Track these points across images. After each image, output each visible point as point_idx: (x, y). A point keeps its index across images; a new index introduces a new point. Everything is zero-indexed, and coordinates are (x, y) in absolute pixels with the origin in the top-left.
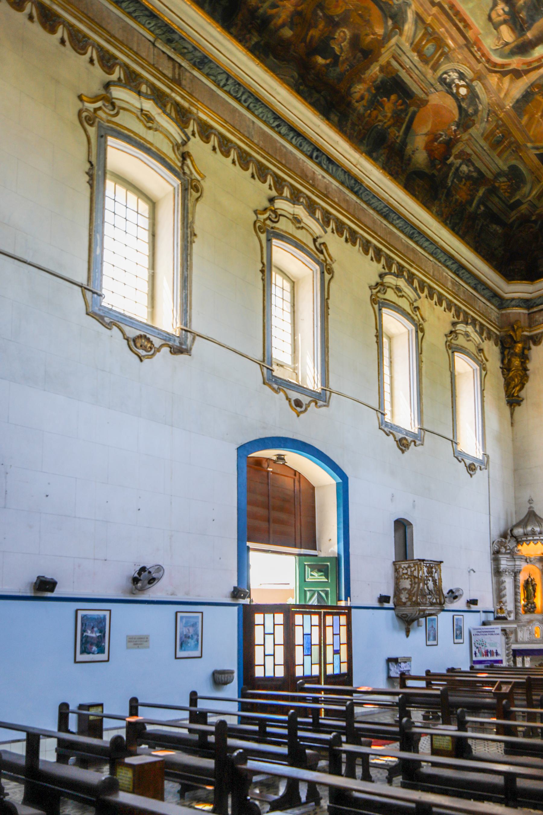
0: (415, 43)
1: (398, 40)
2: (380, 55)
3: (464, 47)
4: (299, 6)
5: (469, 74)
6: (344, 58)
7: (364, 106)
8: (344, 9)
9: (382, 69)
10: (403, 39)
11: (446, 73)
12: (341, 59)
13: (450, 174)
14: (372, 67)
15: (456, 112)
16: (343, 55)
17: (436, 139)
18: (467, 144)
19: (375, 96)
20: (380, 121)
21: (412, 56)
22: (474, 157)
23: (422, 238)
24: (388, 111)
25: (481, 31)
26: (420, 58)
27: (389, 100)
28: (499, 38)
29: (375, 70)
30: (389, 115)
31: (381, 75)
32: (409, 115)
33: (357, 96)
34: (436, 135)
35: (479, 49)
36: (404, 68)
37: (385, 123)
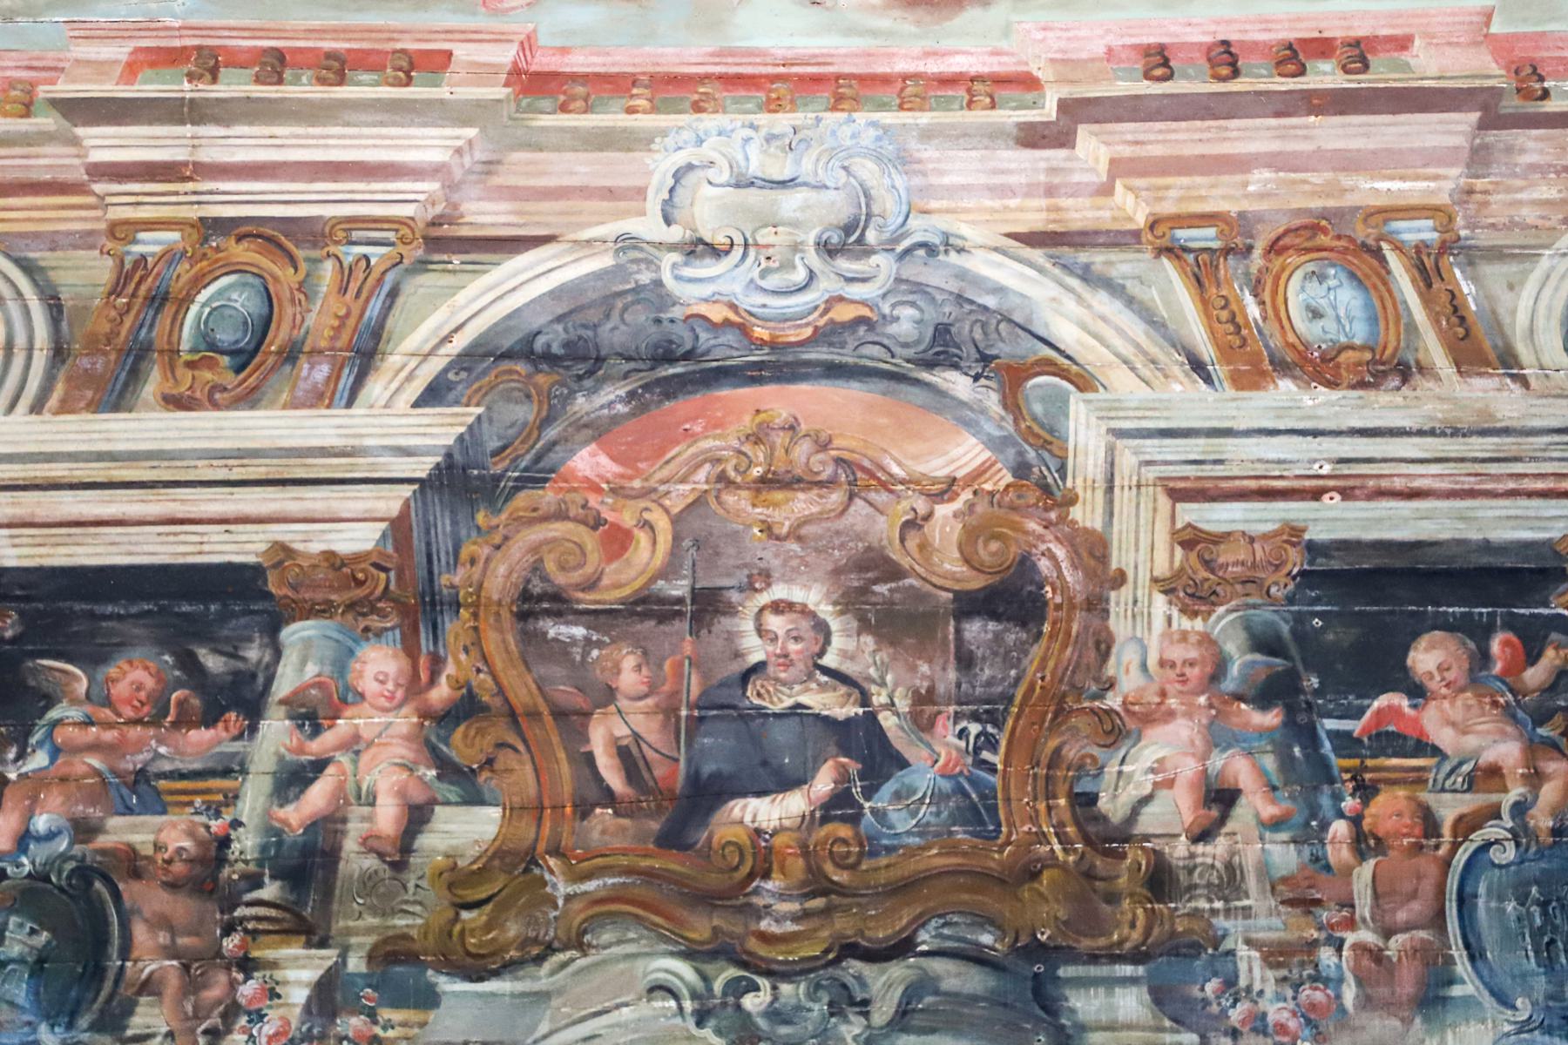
0: (1207, 351)
1: (1108, 411)
3: (1492, 136)
4: (433, 681)
6: (903, 705)
7: (1276, 824)
8: (662, 524)
10: (1123, 384)
12: (887, 721)
14: (1119, 625)
16: (880, 698)
19: (1300, 729)
20: (1466, 826)
21: (1280, 412)
24: (1471, 742)
26: (1332, 385)
27: (1417, 692)
30: (1507, 751)
31: (1223, 623)
36: (1316, 494)
37: (1520, 809)
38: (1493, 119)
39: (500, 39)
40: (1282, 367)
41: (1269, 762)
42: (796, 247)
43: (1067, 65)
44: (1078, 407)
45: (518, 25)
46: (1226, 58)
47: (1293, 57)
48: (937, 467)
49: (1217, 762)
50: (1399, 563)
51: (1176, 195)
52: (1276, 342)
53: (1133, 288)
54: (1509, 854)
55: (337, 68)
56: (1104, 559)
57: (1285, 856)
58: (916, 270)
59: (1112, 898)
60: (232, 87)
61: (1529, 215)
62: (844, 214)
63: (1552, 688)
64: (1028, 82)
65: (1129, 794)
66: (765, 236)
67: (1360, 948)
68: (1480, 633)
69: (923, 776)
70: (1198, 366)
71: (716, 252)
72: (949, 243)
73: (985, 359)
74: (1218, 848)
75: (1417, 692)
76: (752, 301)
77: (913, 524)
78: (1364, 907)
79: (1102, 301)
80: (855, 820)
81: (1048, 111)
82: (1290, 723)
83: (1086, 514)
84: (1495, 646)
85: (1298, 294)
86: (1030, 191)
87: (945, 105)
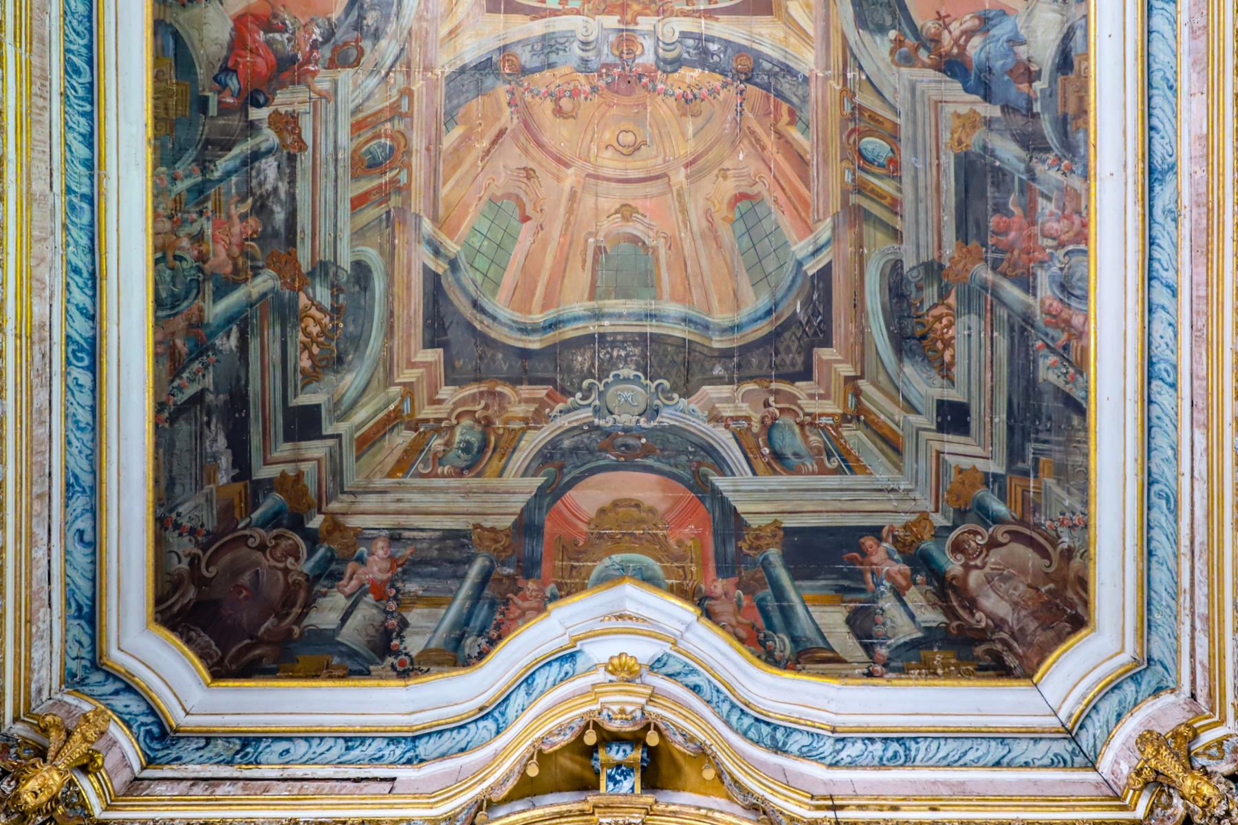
13: (236, 151)
17: (269, 28)
22: (305, 161)
23: (83, 114)
34: (275, 16)
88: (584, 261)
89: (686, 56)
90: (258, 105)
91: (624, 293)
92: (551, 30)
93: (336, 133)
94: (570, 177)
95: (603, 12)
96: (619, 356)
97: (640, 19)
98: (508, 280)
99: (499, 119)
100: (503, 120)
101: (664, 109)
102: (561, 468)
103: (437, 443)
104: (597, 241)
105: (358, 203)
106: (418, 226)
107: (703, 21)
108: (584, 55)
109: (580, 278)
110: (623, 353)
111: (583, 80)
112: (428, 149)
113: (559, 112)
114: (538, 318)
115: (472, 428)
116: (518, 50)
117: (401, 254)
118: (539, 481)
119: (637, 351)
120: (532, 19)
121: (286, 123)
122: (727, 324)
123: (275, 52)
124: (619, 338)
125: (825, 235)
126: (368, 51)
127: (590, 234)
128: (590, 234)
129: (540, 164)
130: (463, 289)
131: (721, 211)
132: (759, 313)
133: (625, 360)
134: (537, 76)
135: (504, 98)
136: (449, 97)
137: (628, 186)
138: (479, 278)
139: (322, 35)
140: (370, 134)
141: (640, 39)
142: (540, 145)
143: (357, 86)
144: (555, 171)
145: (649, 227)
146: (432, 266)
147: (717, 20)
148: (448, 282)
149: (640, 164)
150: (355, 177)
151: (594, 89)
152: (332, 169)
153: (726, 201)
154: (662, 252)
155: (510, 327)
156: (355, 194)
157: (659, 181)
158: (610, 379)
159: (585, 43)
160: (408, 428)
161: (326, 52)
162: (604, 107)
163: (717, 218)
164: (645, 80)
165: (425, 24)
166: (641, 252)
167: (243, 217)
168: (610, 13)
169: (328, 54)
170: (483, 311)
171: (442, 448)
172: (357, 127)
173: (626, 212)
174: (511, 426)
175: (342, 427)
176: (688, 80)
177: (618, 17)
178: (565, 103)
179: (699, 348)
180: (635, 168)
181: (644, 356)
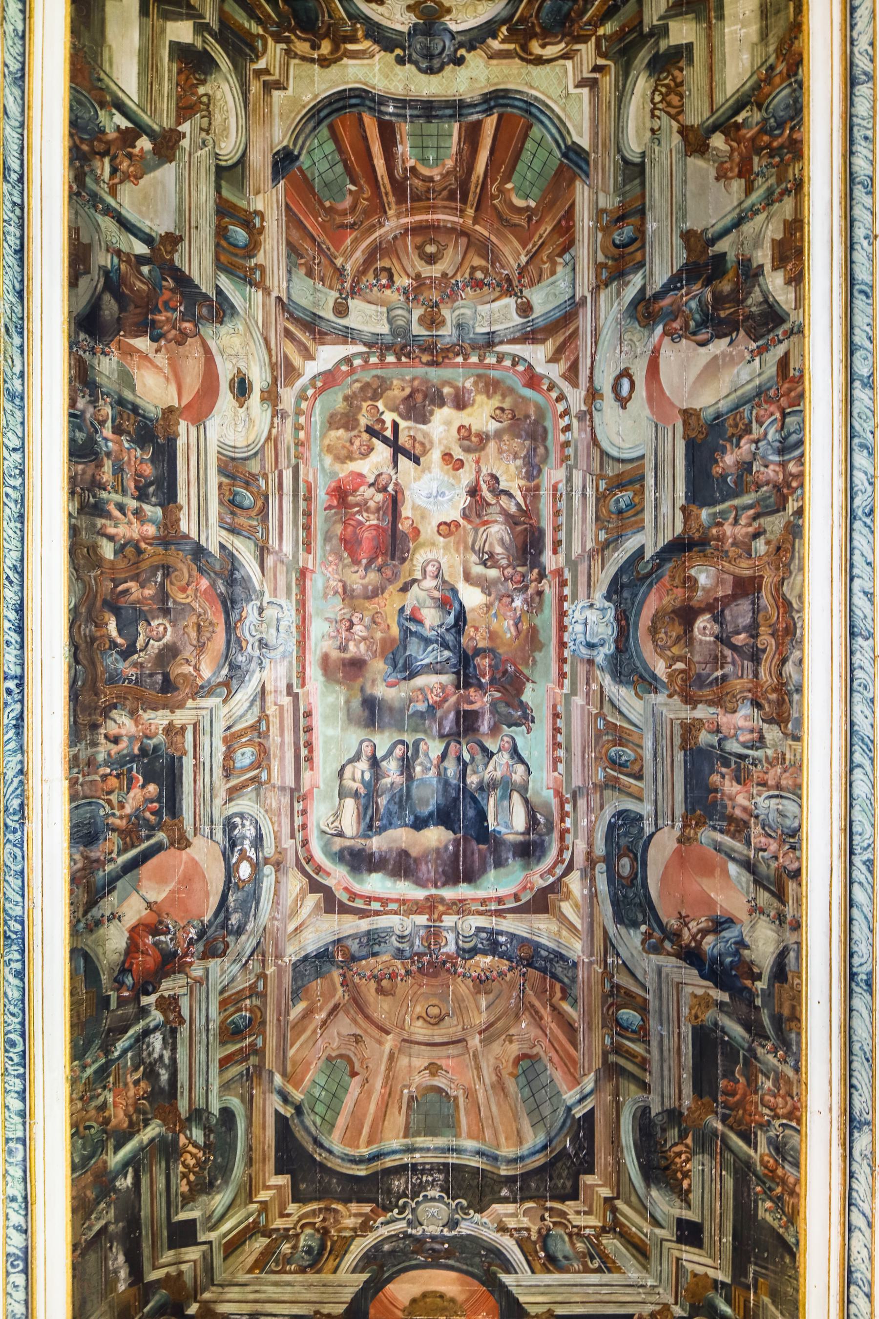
0: (233, 730)
1: (217, 707)
2: (181, 705)
3: (288, 791)
5: (269, 849)
6: (140, 660)
7: (109, 755)
9: (169, 729)
10: (224, 710)
11: (242, 816)
14: (161, 712)
15: (214, 901)
17: (155, 932)
18: (191, 987)
19: (133, 758)
20: (109, 802)
21: (217, 748)
24: (130, 801)
25: (322, 785)
27: (143, 786)
28: (337, 815)
29: (158, 719)
30: (128, 810)
31: (161, 738)
32: (152, 841)
33: (112, 728)
34: (161, 922)
35: (304, 812)
36: (195, 758)
37: (113, 815)
38: (292, 791)
39: (314, 565)
40: (229, 748)
41: (125, 752)
42: (261, 633)
43: (307, 694)
44: (219, 700)
45: (317, 570)
46: (309, 730)
47: (309, 745)
48: (203, 667)
49: (125, 739)
50: (177, 780)
51: (274, 722)
52: (236, 746)
53: (250, 712)
54: (102, 813)
55: (307, 528)
56: (178, 708)
57: (101, 757)
58: (255, 660)
59: (90, 715)
60: (302, 505)
61: (268, 801)
62: (270, 644)
63: (144, 819)
64: (303, 685)
65: (117, 717)
66: (264, 625)
67: (78, 778)
68: (159, 800)
69: (121, 666)
70: (229, 728)
71: (260, 614)
72: (262, 668)
73: (231, 678)
74: (102, 740)
75: (143, 786)
76: (247, 622)
77: (187, 661)
78: (88, 778)
79: (247, 704)
80: (110, 649)
81: (296, 690)
82: (136, 756)
83: (190, 703)
84: (155, 804)
85: (248, 750)
86: (276, 687)
87: (298, 666)
88: (400, 1108)
89: (480, 946)
90: (148, 994)
91: (431, 1131)
92: (375, 927)
93: (207, 1009)
94: (389, 1042)
95: (415, 913)
96: (427, 1181)
97: (444, 917)
98: (342, 1121)
99: (334, 996)
100: (337, 997)
101: (463, 988)
102: (381, 1267)
103: (286, 1248)
104: (410, 1092)
105: (225, 1062)
106: (271, 1081)
107: (494, 918)
108: (400, 946)
109: (397, 1119)
110: (430, 1179)
111: (400, 967)
112: (279, 1020)
113: (381, 991)
114: (365, 1151)
115: (312, 1236)
116: (349, 942)
117: (258, 1101)
118: (365, 1276)
119: (441, 1177)
120: (360, 918)
121: (169, 1005)
122: (512, 1156)
123: (161, 950)
124: (428, 1167)
125: (588, 1089)
126: (232, 945)
127: (405, 1086)
128: (405, 1086)
129: (366, 1031)
130: (307, 1129)
131: (507, 1068)
132: (537, 1148)
133: (432, 1184)
134: (364, 962)
135: (338, 980)
136: (294, 979)
137: (435, 1048)
138: (318, 1121)
139: (196, 933)
140: (233, 1009)
141: (445, 934)
142: (367, 1017)
143: (223, 972)
144: (377, 1037)
145: (451, 1081)
146: (282, 1110)
147: (505, 918)
148: (295, 1123)
149: (443, 1031)
150: (223, 1043)
151: (408, 973)
152: (204, 1036)
153: (511, 1060)
154: (461, 1100)
155: (343, 1159)
156: (222, 1055)
157: (460, 1045)
158: (421, 1198)
159: (403, 937)
160: (263, 1236)
161: (200, 947)
162: (416, 987)
163: (505, 1074)
164: (448, 965)
165: (276, 923)
166: (445, 1099)
167: (137, 1083)
168: (421, 913)
169: (201, 949)
170: (321, 1146)
171: (289, 1251)
172: (223, 1004)
173: (433, 1069)
174: (343, 1234)
175: (213, 1236)
176: (482, 965)
177: (427, 916)
178: (384, 983)
179: (490, 1175)
180: (439, 1034)
181: (446, 1180)
